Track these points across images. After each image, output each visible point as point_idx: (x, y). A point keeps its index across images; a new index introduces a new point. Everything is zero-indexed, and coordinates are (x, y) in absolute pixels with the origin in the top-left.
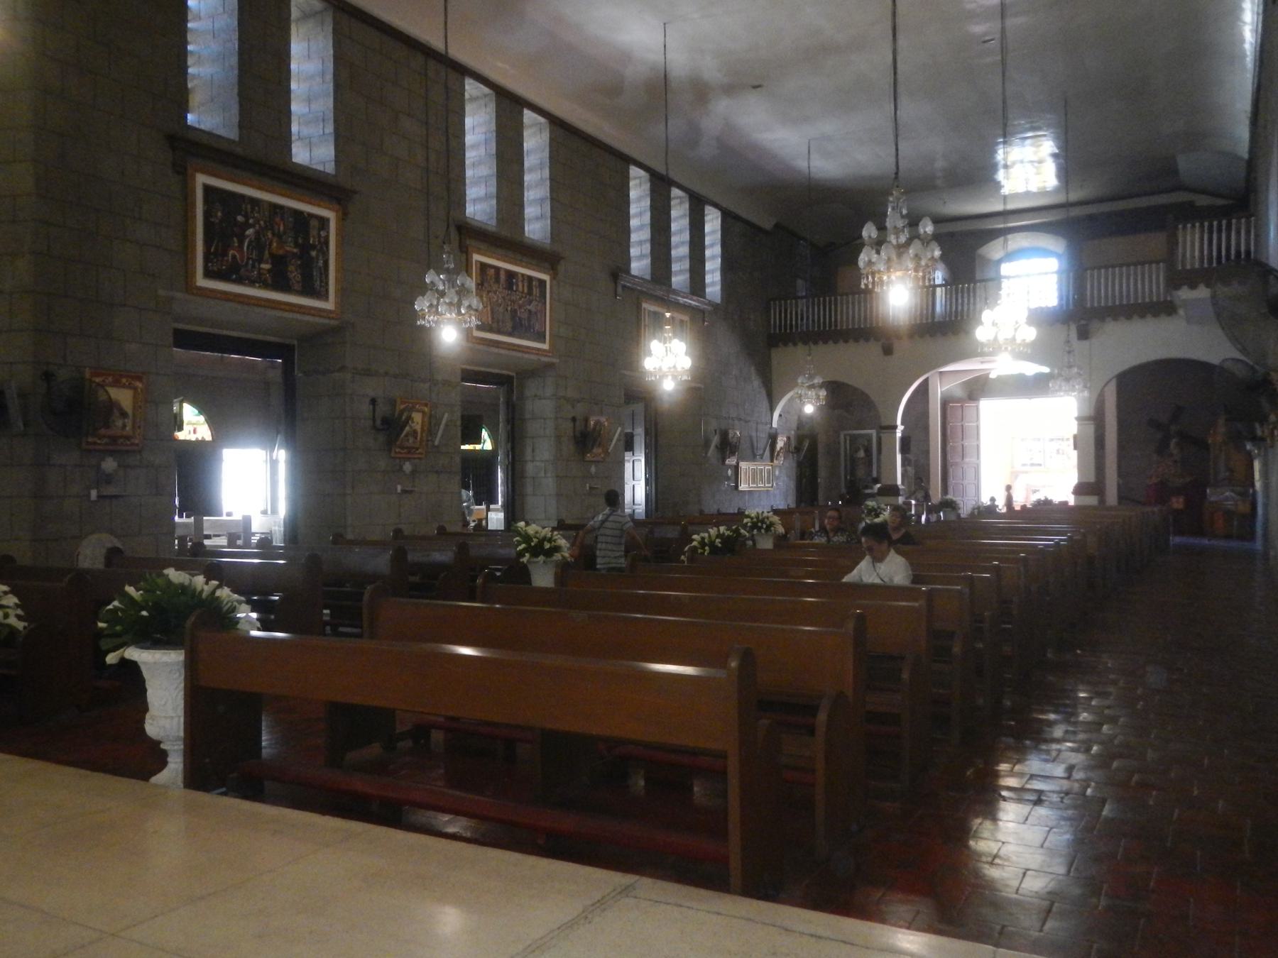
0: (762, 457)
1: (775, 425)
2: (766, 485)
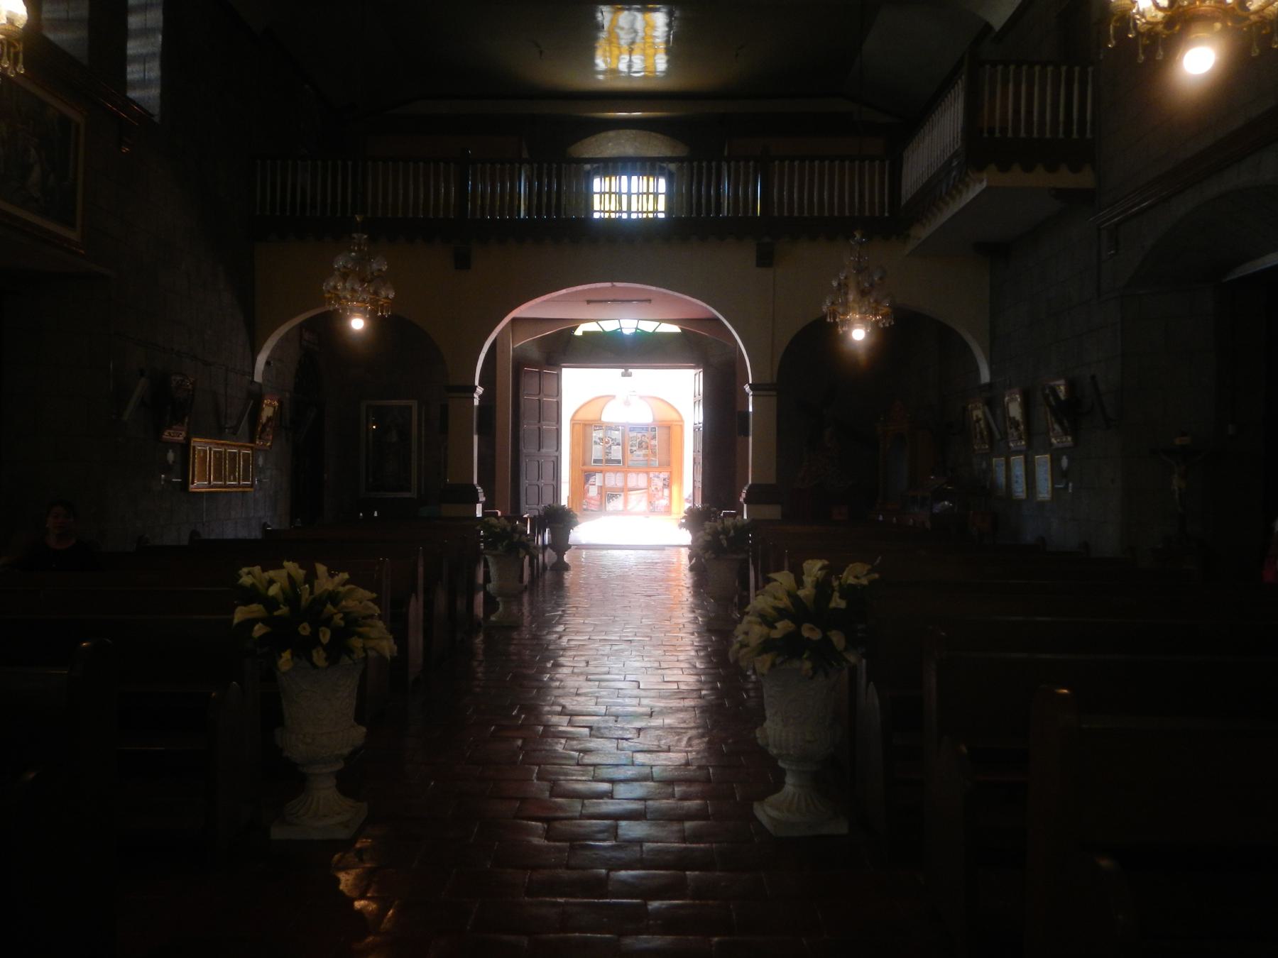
0: (235, 431)
1: (258, 378)
2: (241, 483)
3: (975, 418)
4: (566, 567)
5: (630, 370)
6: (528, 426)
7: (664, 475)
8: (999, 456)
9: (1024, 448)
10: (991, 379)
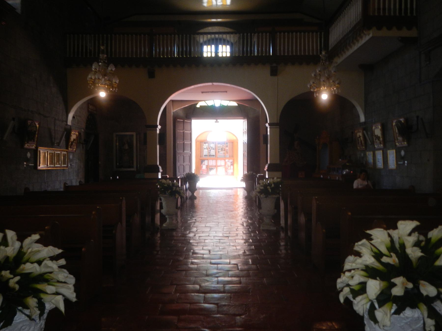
0: (58, 144)
1: (69, 123)
3: (358, 136)
4: (195, 198)
5: (218, 120)
6: (179, 142)
7: (231, 161)
8: (370, 151)
9: (382, 147)
10: (365, 120)
